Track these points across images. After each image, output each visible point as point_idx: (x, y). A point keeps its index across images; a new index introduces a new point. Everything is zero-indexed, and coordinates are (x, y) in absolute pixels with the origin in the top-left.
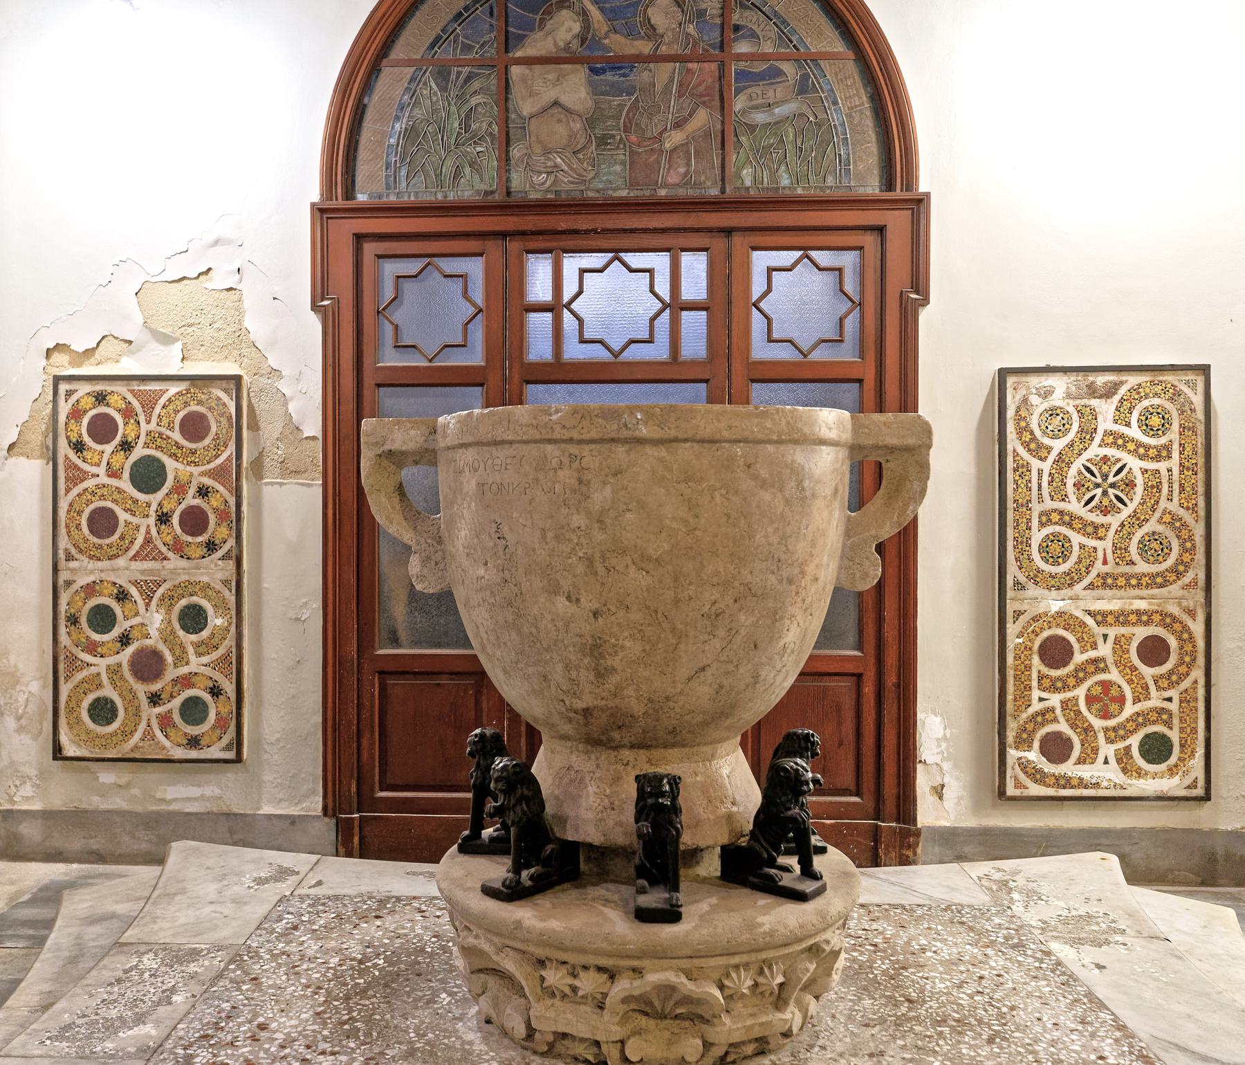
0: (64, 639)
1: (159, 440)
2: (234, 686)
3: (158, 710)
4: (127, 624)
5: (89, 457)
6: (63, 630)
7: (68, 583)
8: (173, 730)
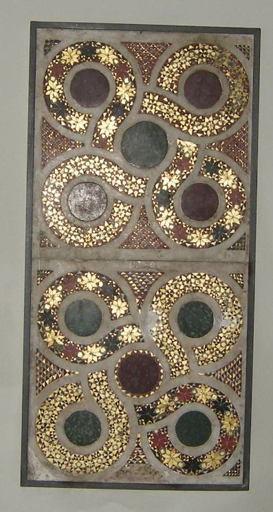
0: (35, 338)
1: (159, 104)
2: (243, 401)
3: (149, 427)
4: (115, 325)
5: (72, 122)
6: (34, 331)
7: (43, 275)
8: (168, 452)
